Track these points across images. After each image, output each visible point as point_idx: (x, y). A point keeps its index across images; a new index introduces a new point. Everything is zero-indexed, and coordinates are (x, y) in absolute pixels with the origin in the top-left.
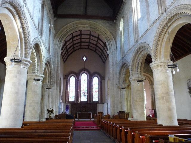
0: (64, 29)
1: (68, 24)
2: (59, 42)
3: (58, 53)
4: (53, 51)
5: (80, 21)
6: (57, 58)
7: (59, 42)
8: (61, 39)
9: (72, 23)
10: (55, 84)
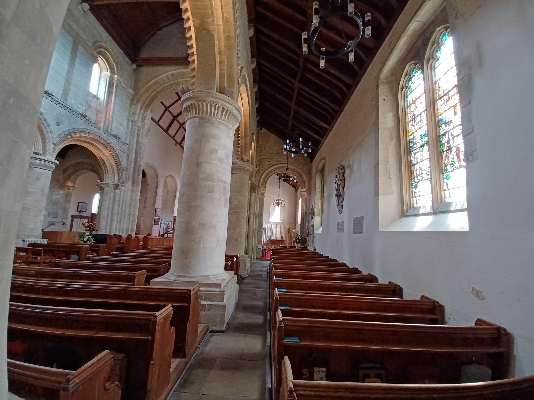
0: (150, 86)
1: (157, 77)
2: (142, 111)
3: (139, 130)
4: (128, 124)
5: (179, 71)
6: (135, 139)
7: (142, 111)
8: (145, 105)
9: (165, 75)
10: (130, 183)
